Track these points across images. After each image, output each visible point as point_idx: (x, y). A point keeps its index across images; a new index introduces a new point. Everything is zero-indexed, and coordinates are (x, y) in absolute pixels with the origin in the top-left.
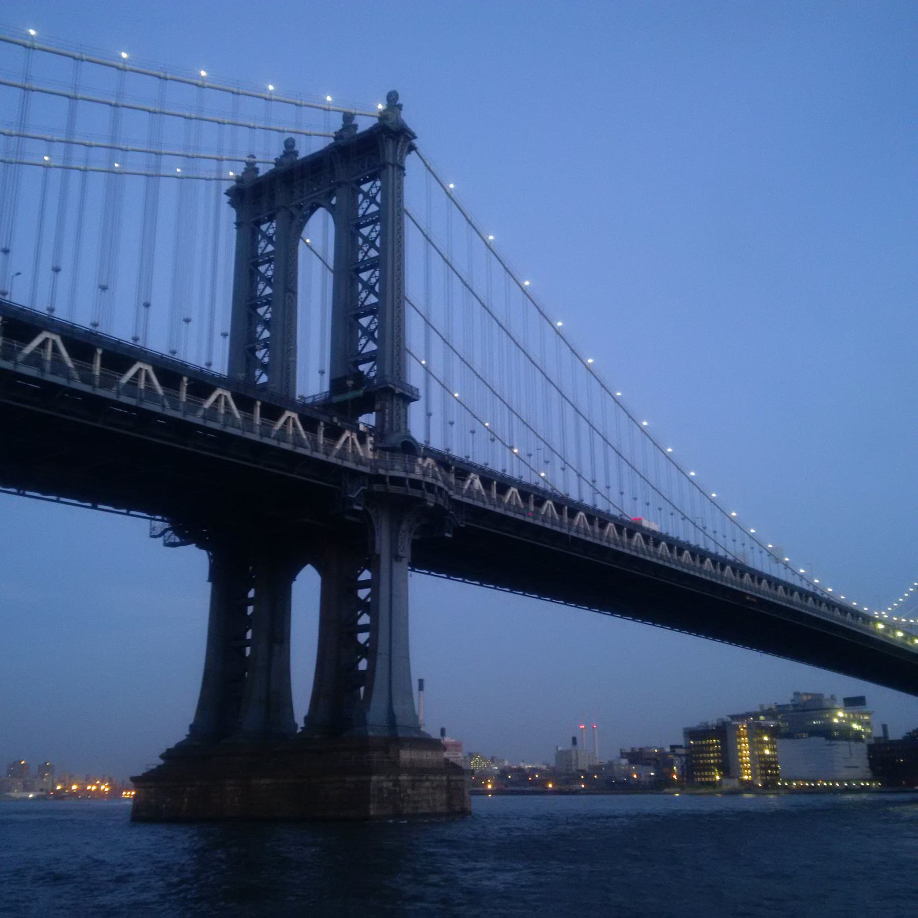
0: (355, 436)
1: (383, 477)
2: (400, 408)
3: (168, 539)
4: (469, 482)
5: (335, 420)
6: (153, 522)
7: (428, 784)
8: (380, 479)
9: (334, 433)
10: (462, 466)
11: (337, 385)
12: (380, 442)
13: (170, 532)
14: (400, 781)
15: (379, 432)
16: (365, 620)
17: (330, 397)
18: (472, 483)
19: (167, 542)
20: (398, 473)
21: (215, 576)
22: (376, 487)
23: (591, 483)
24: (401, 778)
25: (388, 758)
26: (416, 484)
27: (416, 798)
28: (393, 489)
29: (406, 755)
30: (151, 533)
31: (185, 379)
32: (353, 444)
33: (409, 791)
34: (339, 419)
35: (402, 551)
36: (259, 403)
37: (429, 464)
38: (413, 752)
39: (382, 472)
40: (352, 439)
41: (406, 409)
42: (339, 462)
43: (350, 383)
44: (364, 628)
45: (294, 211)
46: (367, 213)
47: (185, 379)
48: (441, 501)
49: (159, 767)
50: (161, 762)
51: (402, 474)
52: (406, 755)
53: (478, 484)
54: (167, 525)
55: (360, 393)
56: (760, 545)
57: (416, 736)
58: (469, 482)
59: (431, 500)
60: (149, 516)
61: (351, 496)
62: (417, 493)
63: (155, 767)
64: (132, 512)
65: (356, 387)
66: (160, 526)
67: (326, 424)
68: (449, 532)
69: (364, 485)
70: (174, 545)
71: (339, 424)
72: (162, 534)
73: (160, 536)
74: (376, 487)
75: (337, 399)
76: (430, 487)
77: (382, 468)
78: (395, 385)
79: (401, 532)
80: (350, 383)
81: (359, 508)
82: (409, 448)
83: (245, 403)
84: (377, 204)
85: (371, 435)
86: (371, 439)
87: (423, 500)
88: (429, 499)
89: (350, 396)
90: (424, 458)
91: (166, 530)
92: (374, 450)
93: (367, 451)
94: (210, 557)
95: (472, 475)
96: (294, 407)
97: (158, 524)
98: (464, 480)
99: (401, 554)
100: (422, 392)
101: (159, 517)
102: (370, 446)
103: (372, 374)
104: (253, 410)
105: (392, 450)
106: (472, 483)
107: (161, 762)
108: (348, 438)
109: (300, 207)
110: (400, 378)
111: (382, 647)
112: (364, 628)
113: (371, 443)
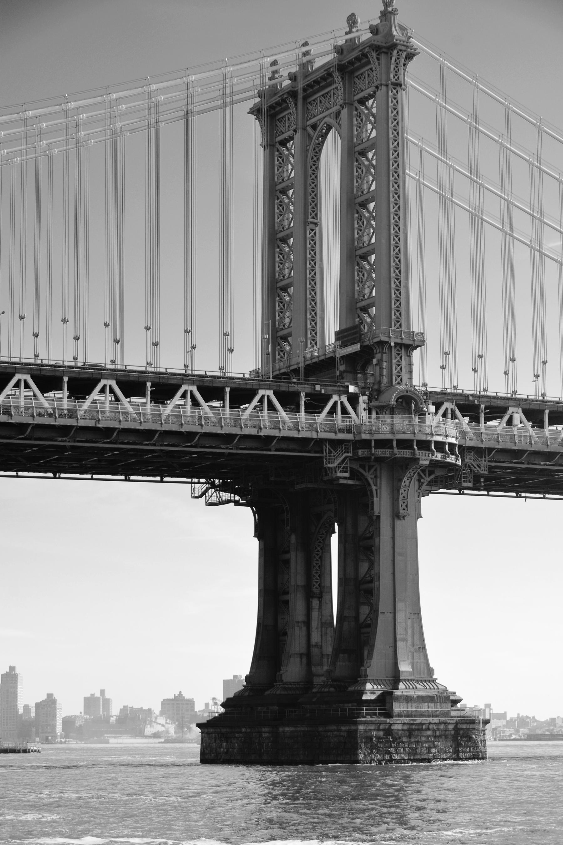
0: (344, 399)
1: (370, 441)
2: (401, 358)
5: (318, 388)
6: (193, 485)
8: (366, 444)
10: (495, 403)
14: (392, 730)
28: (380, 453)
30: (192, 494)
31: (149, 384)
35: (404, 509)
39: (365, 436)
41: (410, 356)
47: (149, 384)
50: (222, 710)
61: (330, 465)
62: (406, 453)
64: (165, 479)
66: (199, 488)
71: (323, 391)
72: (204, 493)
73: (201, 496)
74: (360, 453)
79: (402, 490)
85: (364, 394)
86: (365, 398)
90: (438, 406)
104: (224, 397)
108: (336, 403)
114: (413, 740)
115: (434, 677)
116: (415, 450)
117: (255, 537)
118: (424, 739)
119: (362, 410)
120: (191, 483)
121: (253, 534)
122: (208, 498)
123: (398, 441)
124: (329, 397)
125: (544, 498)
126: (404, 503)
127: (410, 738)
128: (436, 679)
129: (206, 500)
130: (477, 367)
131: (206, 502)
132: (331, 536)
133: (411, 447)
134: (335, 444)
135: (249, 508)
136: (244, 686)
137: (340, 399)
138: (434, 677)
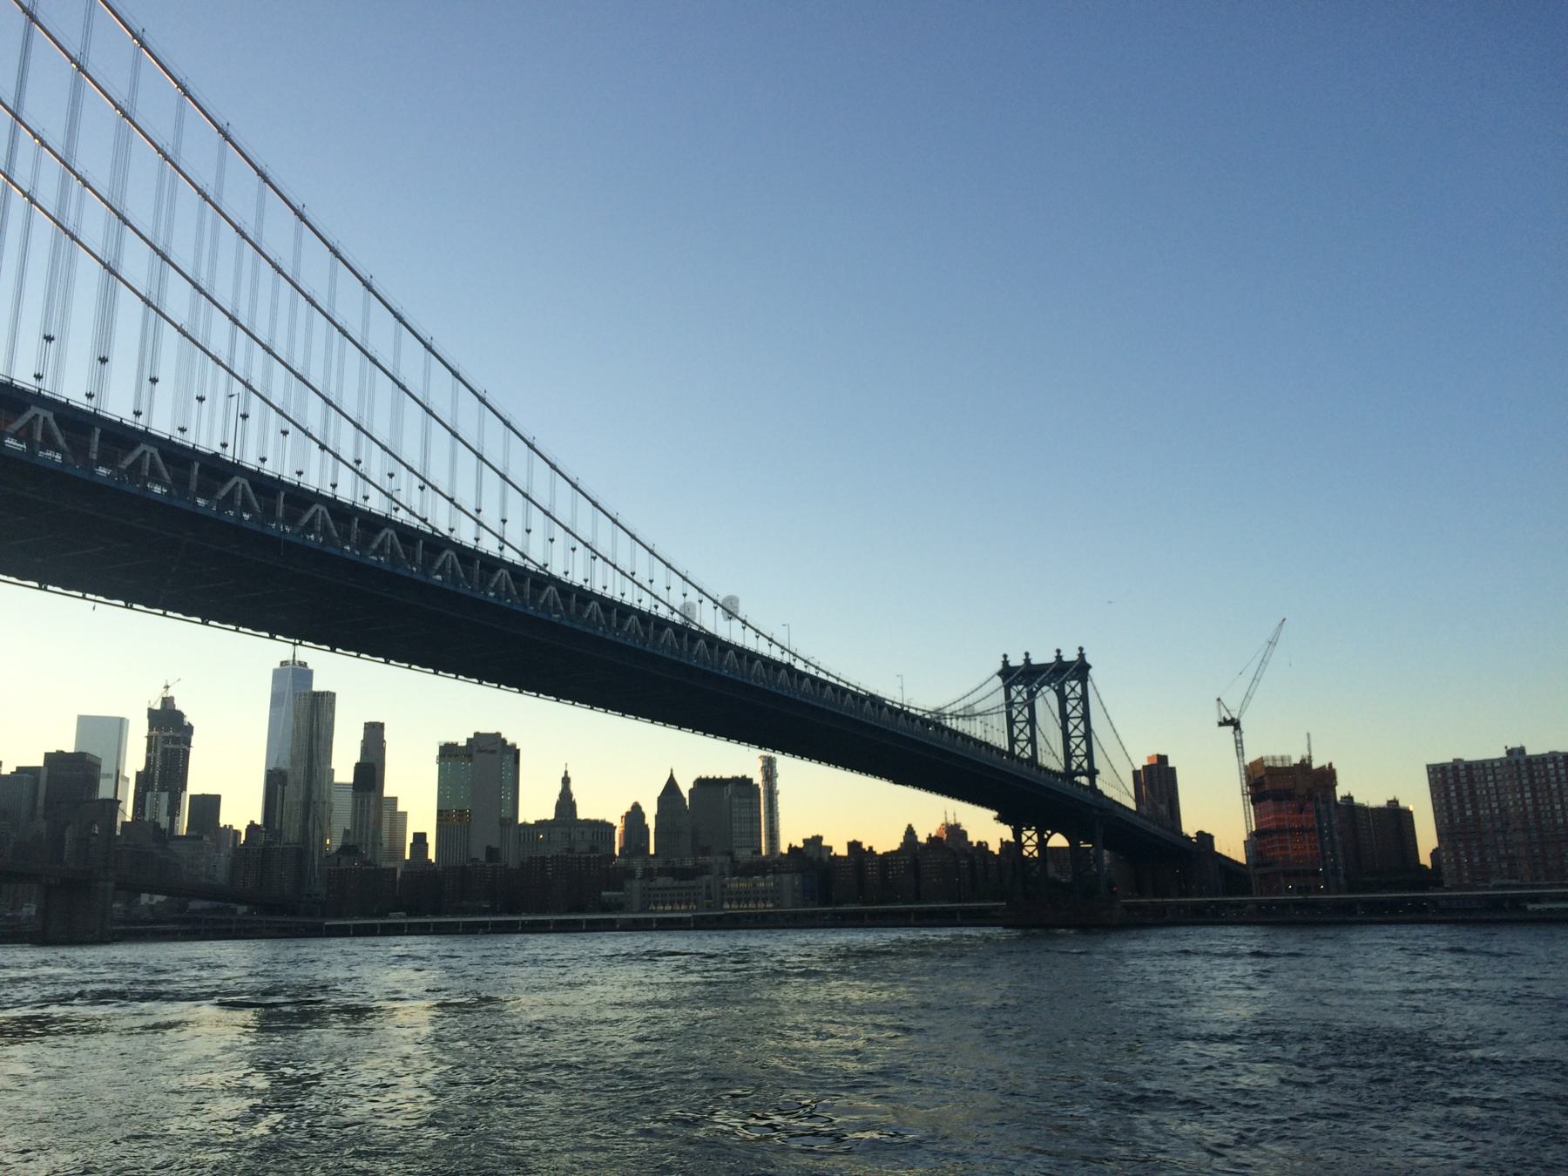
23: (354, 465)
56: (700, 591)
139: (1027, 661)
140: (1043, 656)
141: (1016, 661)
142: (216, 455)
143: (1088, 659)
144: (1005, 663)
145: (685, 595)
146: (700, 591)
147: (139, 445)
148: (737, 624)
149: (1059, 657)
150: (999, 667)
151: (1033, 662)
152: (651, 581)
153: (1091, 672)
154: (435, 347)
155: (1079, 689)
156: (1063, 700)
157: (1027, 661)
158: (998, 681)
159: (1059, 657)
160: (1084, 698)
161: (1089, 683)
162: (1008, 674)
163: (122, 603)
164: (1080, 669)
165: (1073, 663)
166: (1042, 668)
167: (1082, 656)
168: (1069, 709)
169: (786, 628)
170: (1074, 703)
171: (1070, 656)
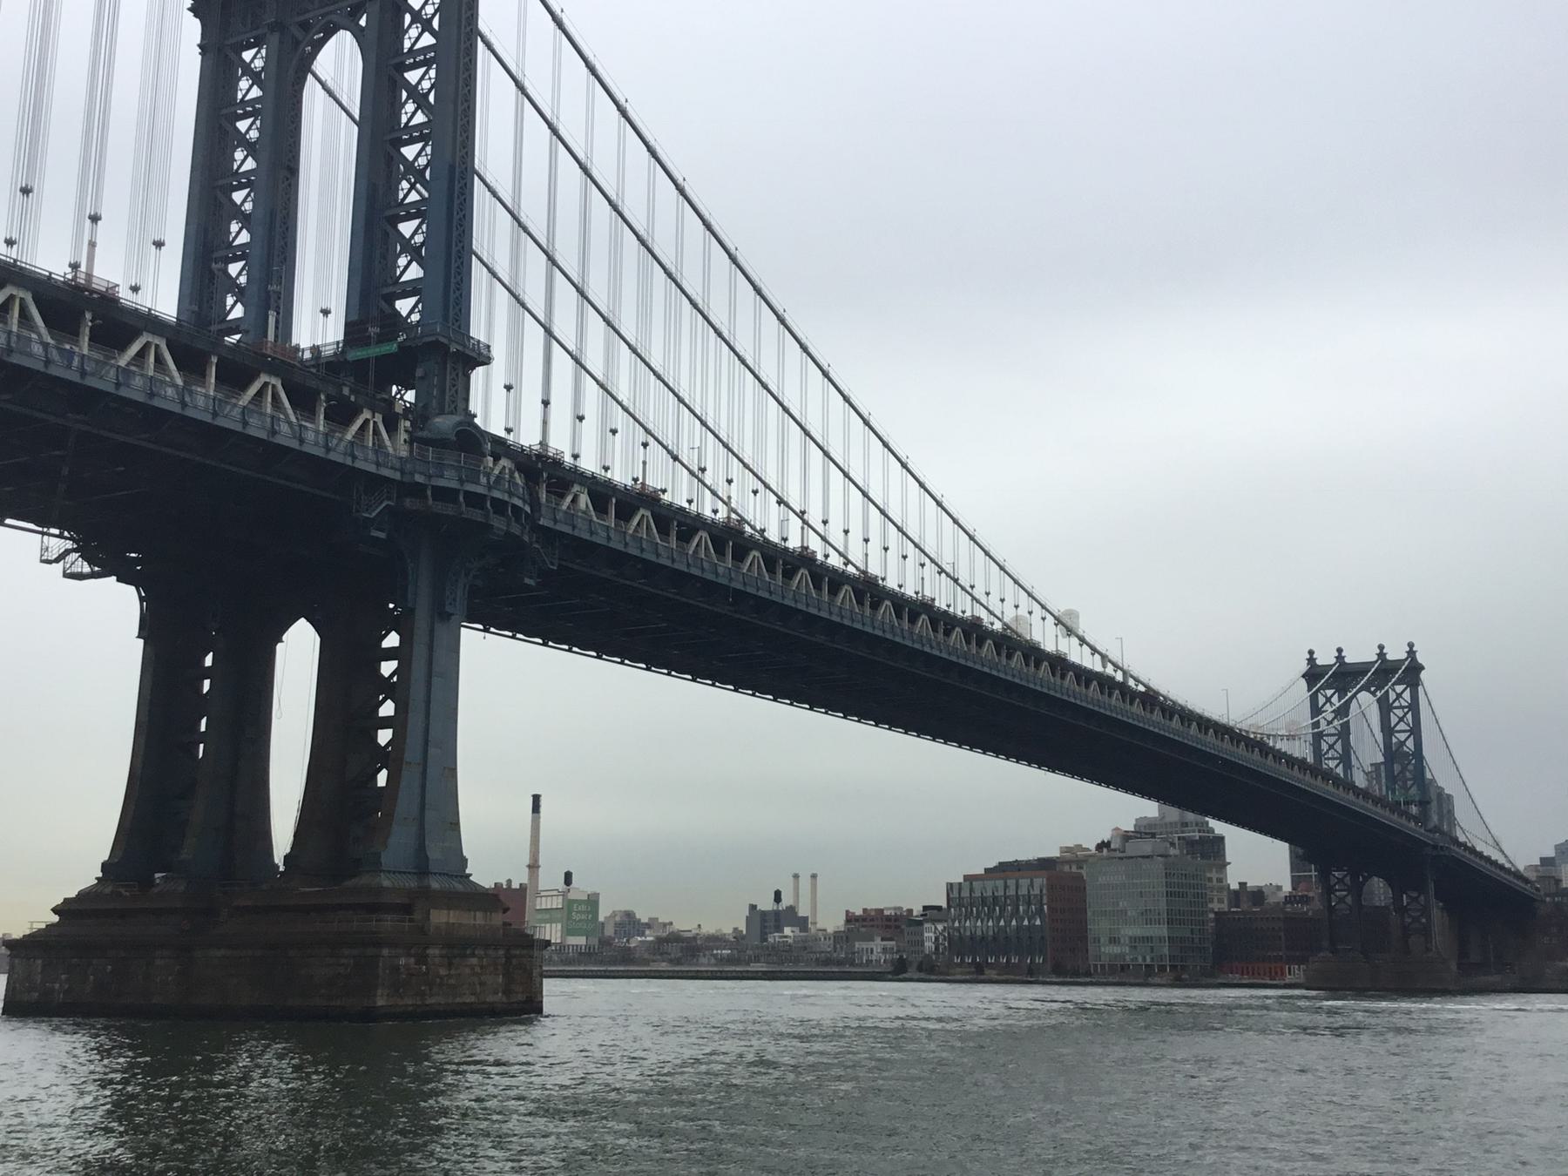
0: (379, 418)
2: (457, 375)
3: (70, 567)
4: (569, 498)
5: (346, 391)
6: (46, 537)
7: (474, 961)
8: (417, 490)
9: (341, 415)
11: (353, 330)
12: (422, 429)
13: (75, 555)
14: (427, 955)
15: (418, 414)
16: (387, 709)
17: (342, 352)
18: (574, 500)
19: (69, 571)
20: (449, 481)
21: (147, 629)
22: (408, 503)
24: (430, 951)
25: (411, 920)
26: (475, 500)
27: (452, 981)
29: (439, 917)
30: (42, 556)
31: (88, 316)
32: (376, 432)
33: (443, 972)
34: (352, 391)
35: (451, 604)
36: (214, 360)
37: (504, 467)
38: (451, 912)
39: (419, 478)
40: (375, 423)
42: (349, 461)
43: (373, 331)
44: (386, 723)
45: (298, 33)
46: (417, 47)
47: (88, 316)
48: (516, 529)
49: (50, 927)
50: (56, 919)
51: (454, 485)
52: (439, 917)
53: (584, 500)
54: (69, 545)
55: (394, 347)
56: (1043, 607)
57: (459, 887)
58: (569, 498)
59: (498, 523)
60: (40, 529)
61: (367, 515)
62: (476, 515)
63: (43, 926)
65: (382, 339)
66: (57, 545)
67: (328, 398)
68: (531, 578)
69: (389, 499)
70: (80, 576)
73: (57, 560)
74: (408, 503)
75: (356, 354)
76: (500, 507)
77: (421, 473)
78: (450, 339)
80: (373, 331)
81: (382, 535)
82: (471, 440)
83: (191, 362)
84: (433, 33)
85: (406, 419)
86: (408, 424)
87: (487, 527)
88: (496, 525)
89: (374, 351)
90: (496, 459)
91: (67, 552)
92: (410, 442)
93: (398, 446)
94: (141, 599)
95: (576, 488)
96: (276, 367)
97: (54, 541)
98: (562, 496)
99: (448, 609)
100: (499, 352)
101: (56, 531)
102: (403, 436)
103: (415, 317)
104: (205, 371)
105: (440, 443)
106: (574, 500)
107: (56, 919)
108: (366, 421)
109: (305, 27)
110: (459, 327)
111: (412, 753)
112: (386, 723)
113: (406, 431)
114: (453, 972)
115: (467, 871)
116: (489, 511)
117: (138, 637)
118: (467, 971)
119: (402, 442)
120: (43, 534)
121: (136, 633)
122: (68, 566)
123: (468, 494)
124: (354, 412)
125: (513, 637)
126: (451, 593)
127: (450, 970)
128: (471, 875)
129: (64, 568)
130: (510, 425)
131: (64, 572)
132: (276, 645)
133: (483, 508)
134: (375, 483)
135: (132, 589)
136: (97, 878)
137: (374, 417)
138: (467, 871)
139: (1340, 658)
140: (1360, 653)
141: (1325, 658)
142: (682, 509)
143: (1420, 659)
144: (1311, 660)
145: (1017, 607)
146: (1043, 607)
147: (639, 509)
148: (1075, 641)
149: (1381, 655)
150: (1304, 667)
151: (1347, 660)
152: (988, 594)
153: (1423, 675)
154: (832, 375)
155: (1407, 695)
156: (1385, 707)
157: (1340, 658)
158: (1303, 683)
159: (1381, 655)
160: (1414, 707)
161: (1420, 688)
162: (1313, 674)
163: (594, 654)
164: (1411, 671)
165: (1401, 662)
166: (1359, 670)
167: (1411, 653)
168: (1394, 720)
169: (1119, 640)
170: (1400, 713)
171: (1396, 653)
